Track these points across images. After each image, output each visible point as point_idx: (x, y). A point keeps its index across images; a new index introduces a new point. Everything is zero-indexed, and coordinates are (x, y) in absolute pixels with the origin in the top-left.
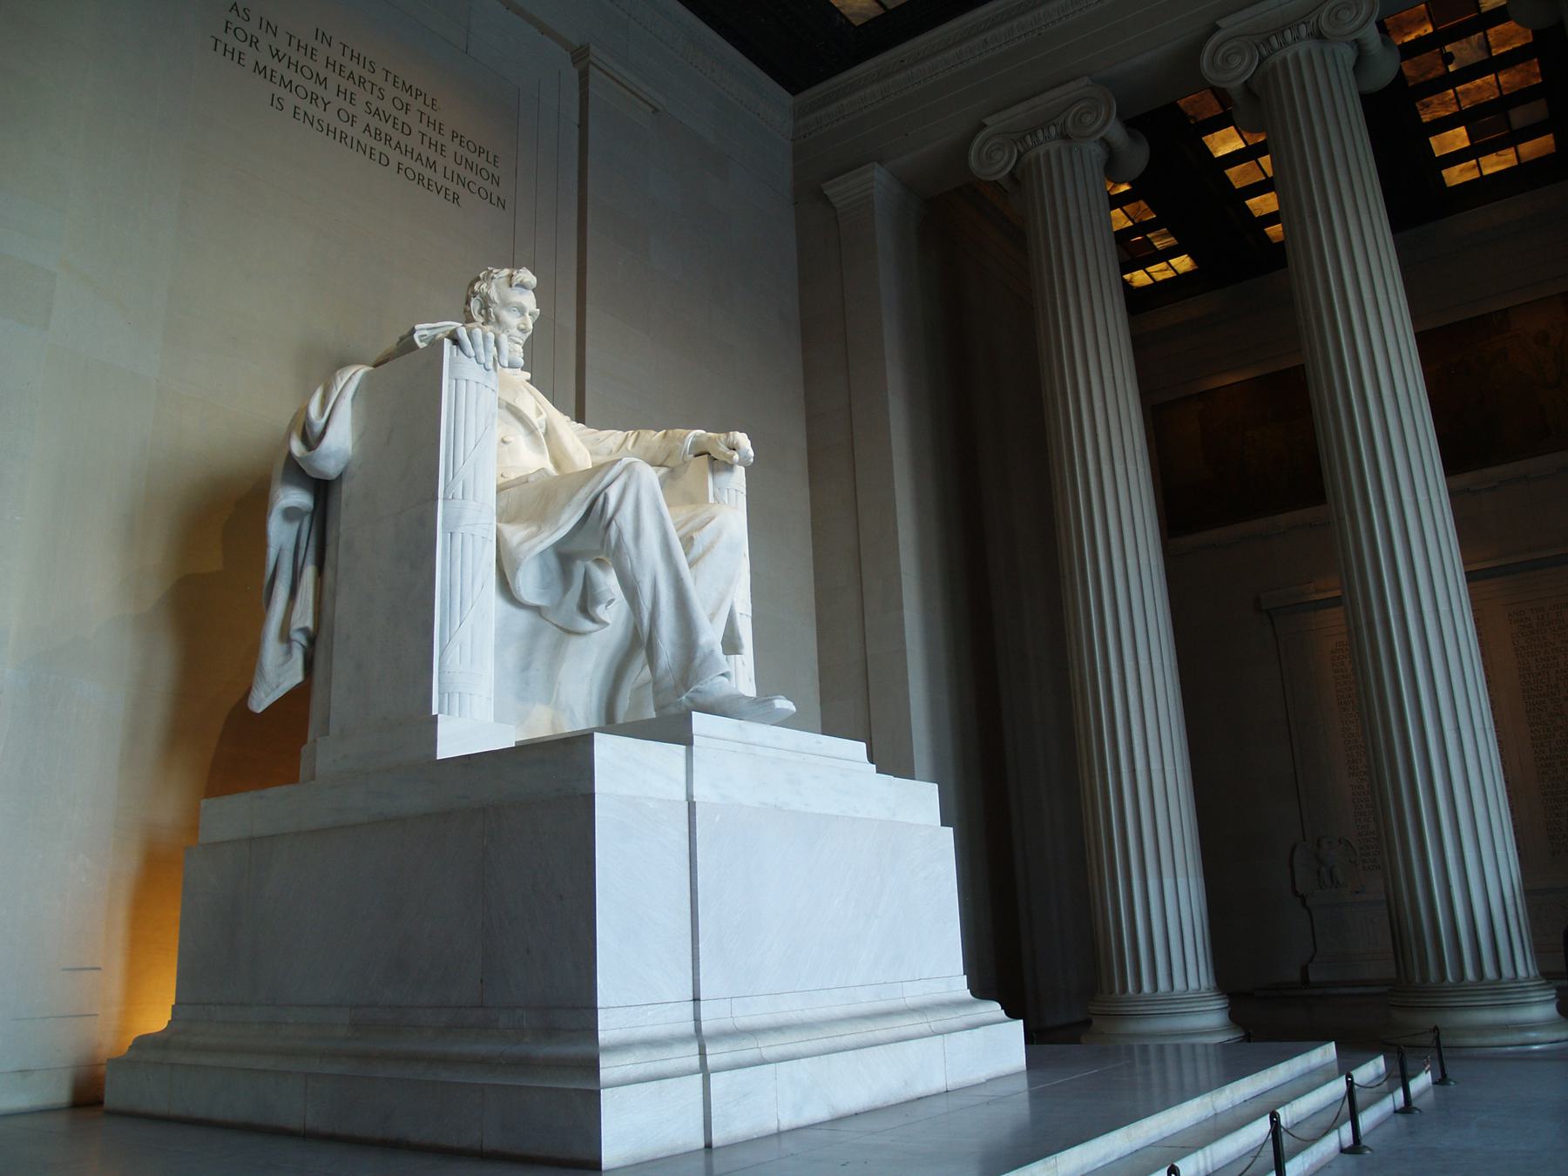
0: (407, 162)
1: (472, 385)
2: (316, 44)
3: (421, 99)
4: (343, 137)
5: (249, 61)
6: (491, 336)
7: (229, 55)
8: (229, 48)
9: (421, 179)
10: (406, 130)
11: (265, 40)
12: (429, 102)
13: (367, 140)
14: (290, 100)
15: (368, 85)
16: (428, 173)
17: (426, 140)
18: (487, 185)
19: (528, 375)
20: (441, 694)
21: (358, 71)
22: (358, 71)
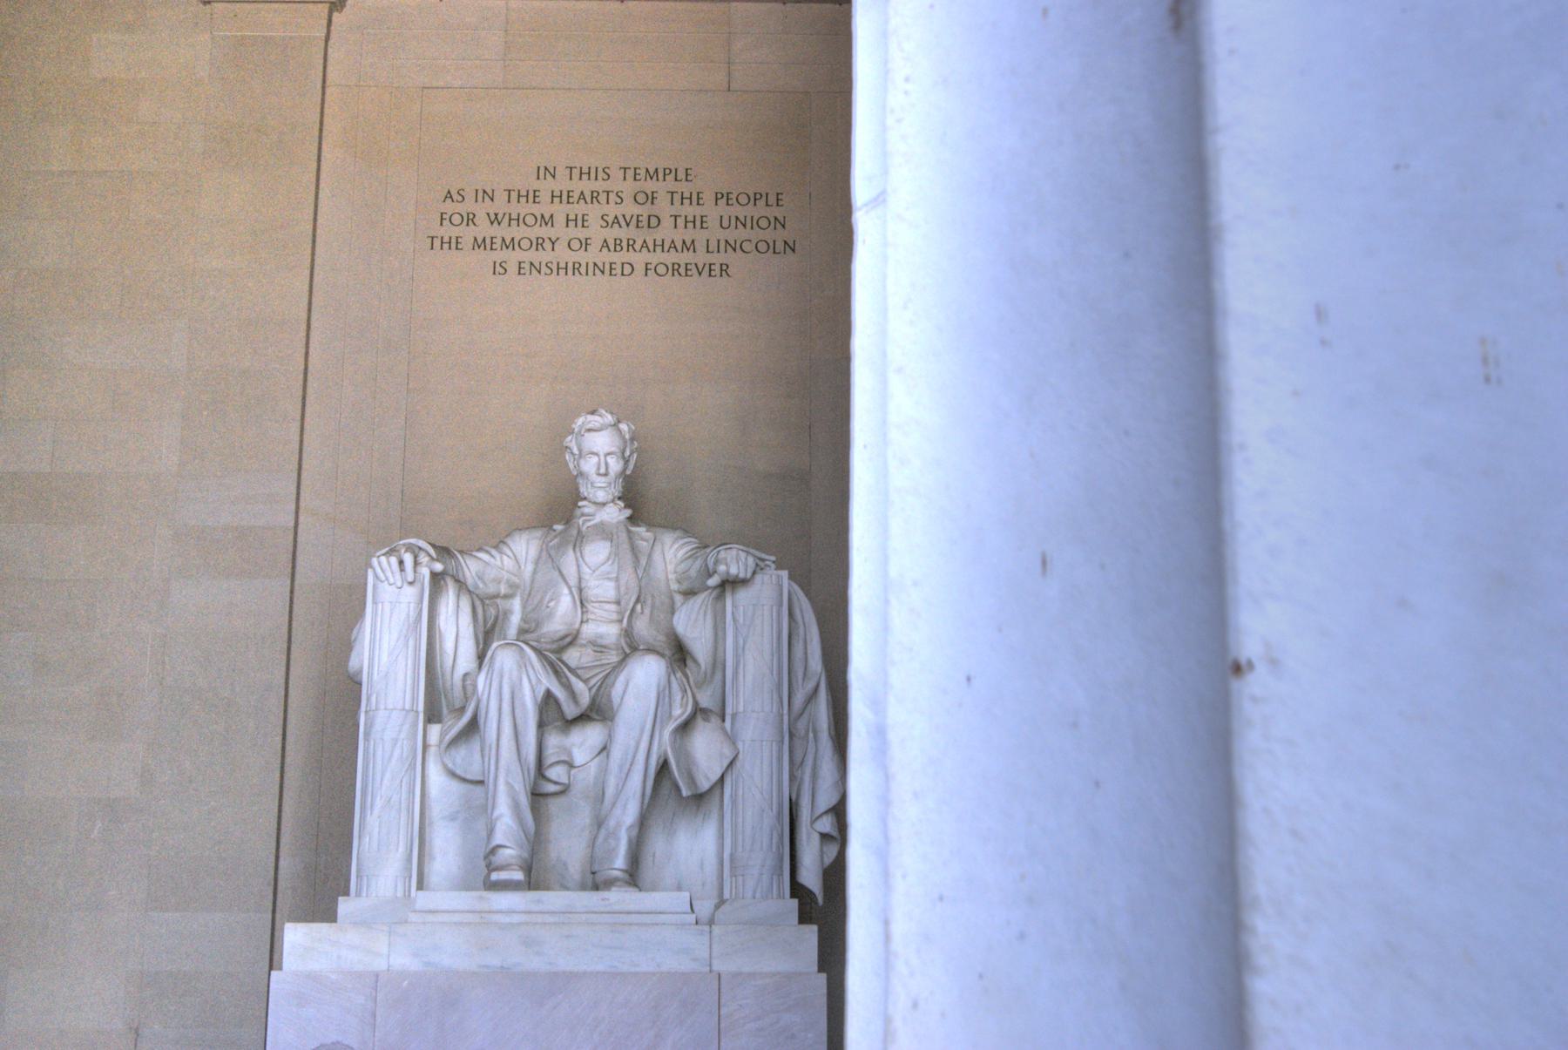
0: (657, 257)
1: (387, 607)
2: (536, 185)
3: (670, 178)
4: (576, 268)
5: (467, 242)
6: (394, 560)
7: (446, 246)
8: (446, 239)
9: (675, 269)
10: (654, 222)
11: (482, 210)
12: (681, 175)
13: (606, 257)
14: (513, 257)
15: (603, 198)
16: (684, 258)
17: (681, 221)
18: (769, 235)
19: (628, 512)
20: (359, 876)
21: (587, 186)
22: (587, 186)
